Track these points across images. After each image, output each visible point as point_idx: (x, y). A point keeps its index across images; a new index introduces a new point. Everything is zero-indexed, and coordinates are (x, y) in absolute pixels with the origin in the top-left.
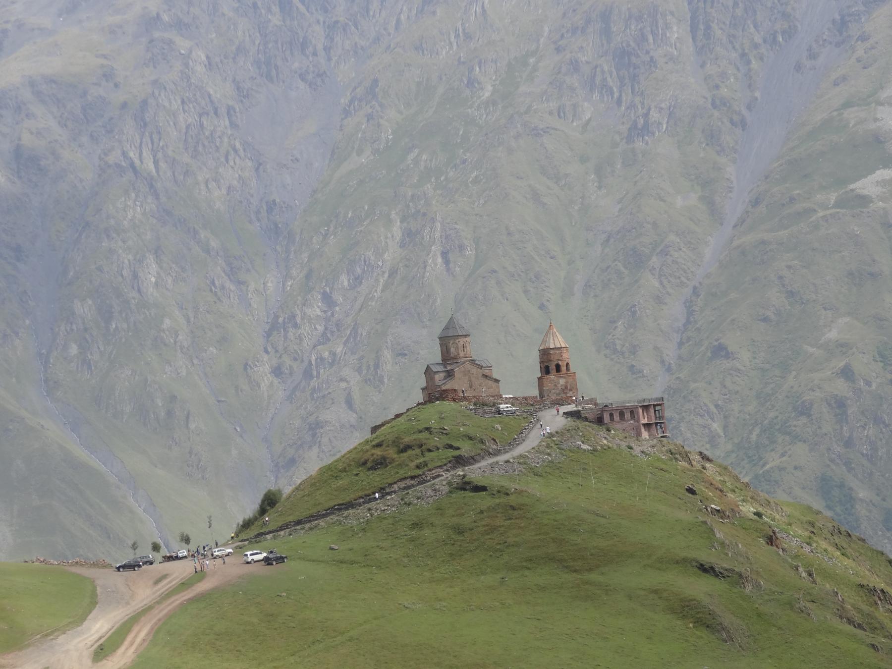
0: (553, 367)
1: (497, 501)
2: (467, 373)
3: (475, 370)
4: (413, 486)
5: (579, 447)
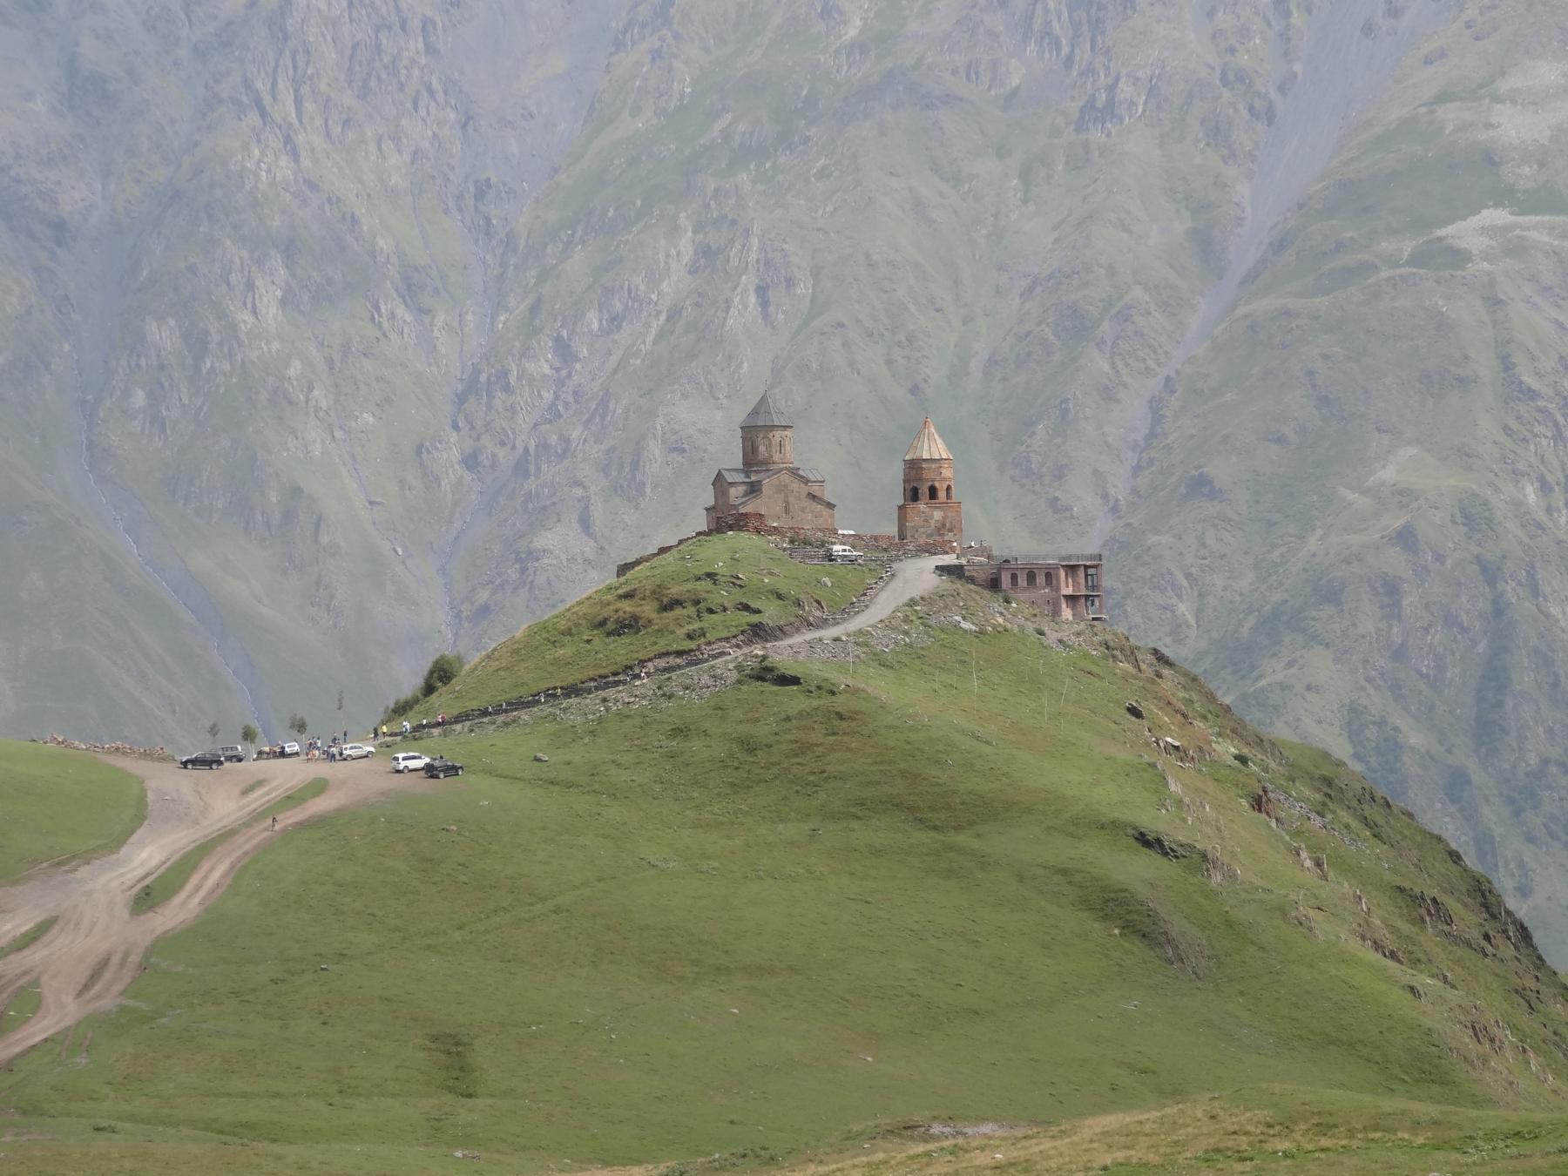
0: (924, 491)
1: (815, 703)
2: (781, 488)
3: (796, 486)
4: (679, 667)
5: (956, 626)
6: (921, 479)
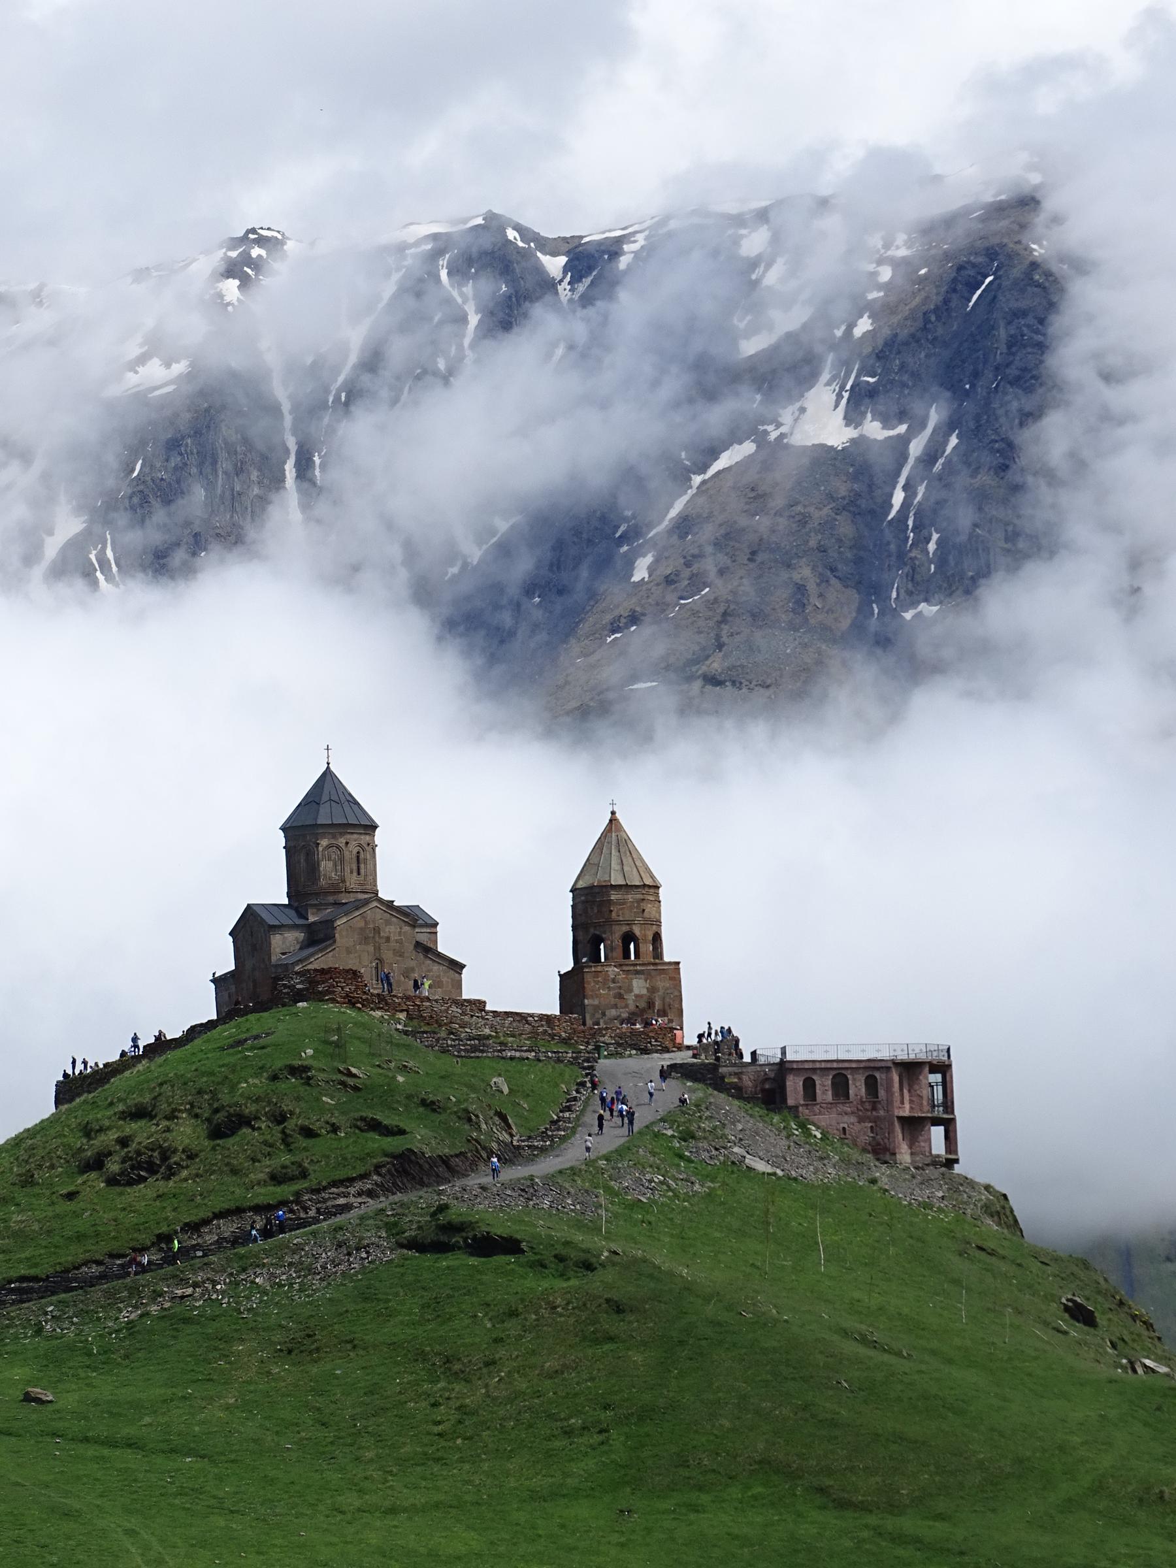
2: (370, 935)
6: (610, 922)
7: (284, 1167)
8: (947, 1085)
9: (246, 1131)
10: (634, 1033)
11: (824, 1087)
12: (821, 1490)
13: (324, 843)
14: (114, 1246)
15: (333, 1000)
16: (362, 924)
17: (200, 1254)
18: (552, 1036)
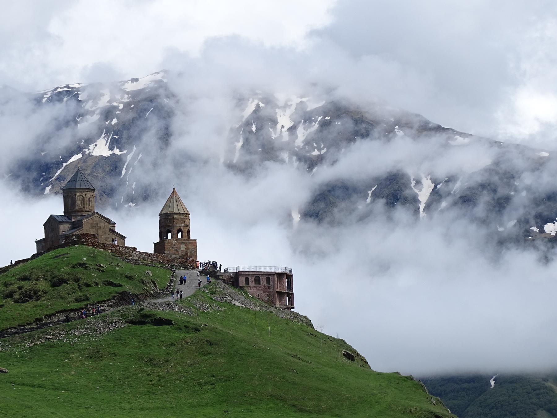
4: (74, 318)
5: (230, 303)
6: (173, 225)
7: (80, 296)
8: (290, 284)
9: (65, 284)
10: (183, 262)
11: (252, 280)
12: (294, 406)
13: (78, 194)
14: (20, 322)
15: (87, 245)
16: (92, 222)
17: (51, 325)
18: (158, 261)
